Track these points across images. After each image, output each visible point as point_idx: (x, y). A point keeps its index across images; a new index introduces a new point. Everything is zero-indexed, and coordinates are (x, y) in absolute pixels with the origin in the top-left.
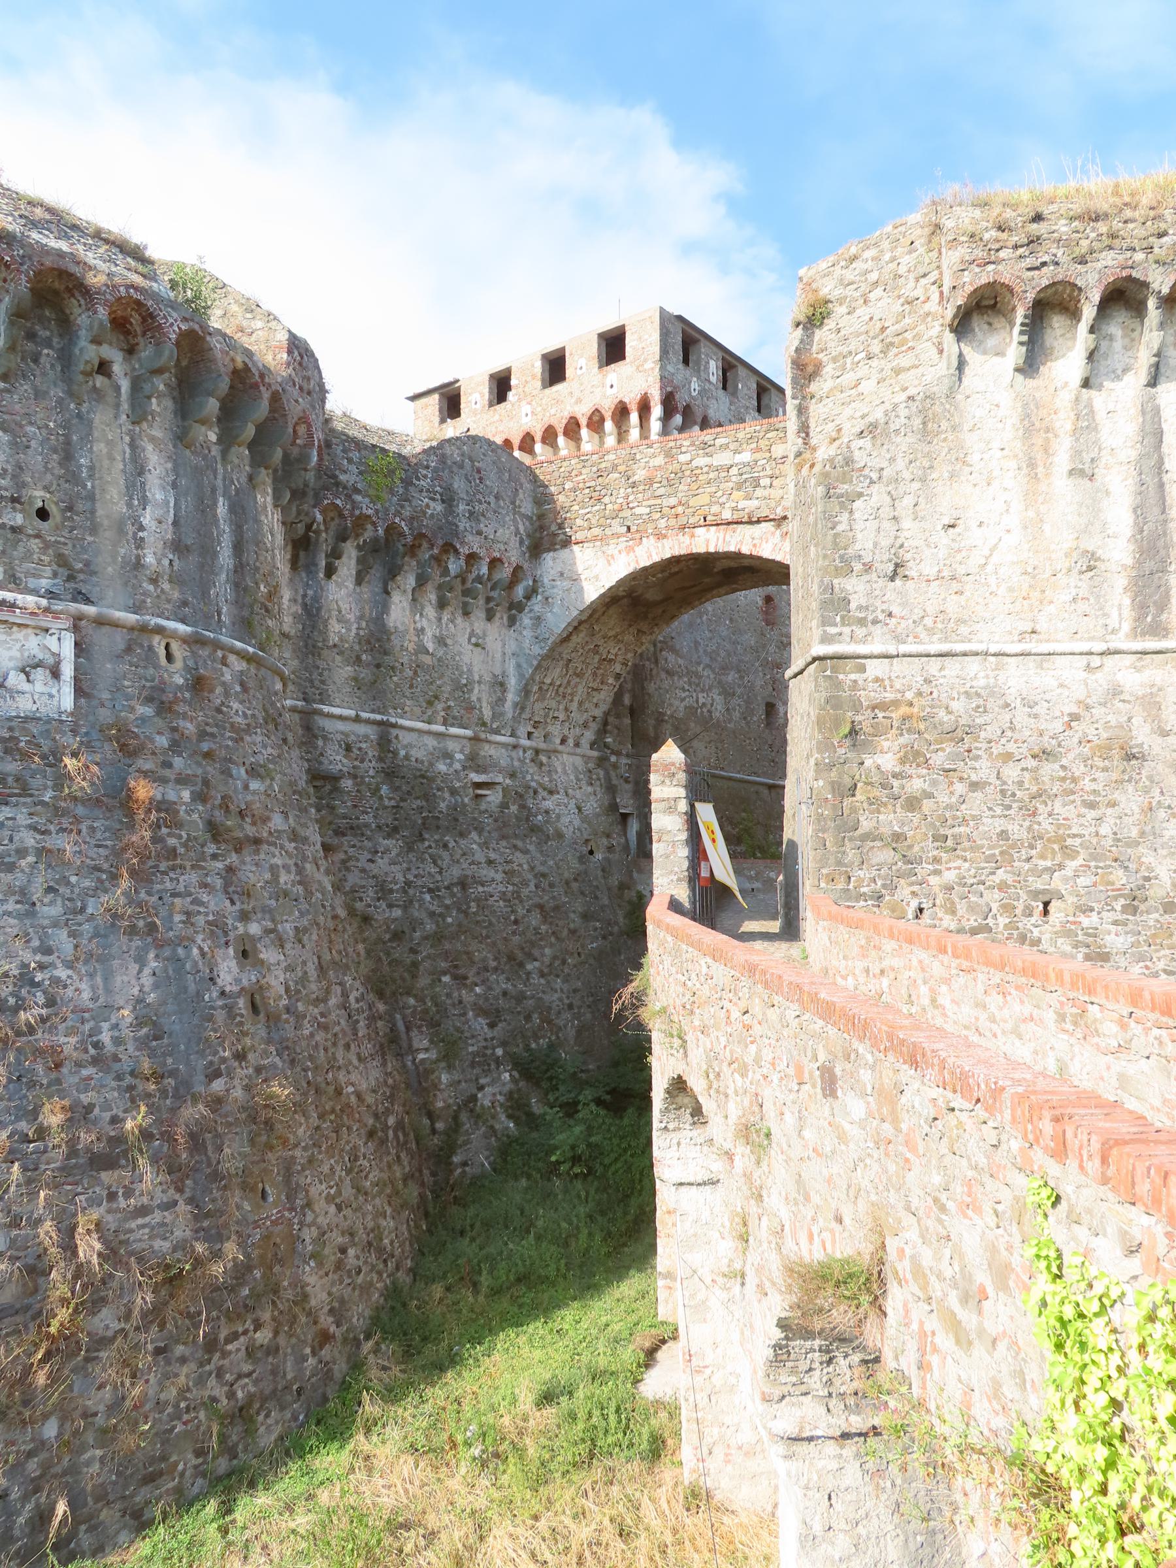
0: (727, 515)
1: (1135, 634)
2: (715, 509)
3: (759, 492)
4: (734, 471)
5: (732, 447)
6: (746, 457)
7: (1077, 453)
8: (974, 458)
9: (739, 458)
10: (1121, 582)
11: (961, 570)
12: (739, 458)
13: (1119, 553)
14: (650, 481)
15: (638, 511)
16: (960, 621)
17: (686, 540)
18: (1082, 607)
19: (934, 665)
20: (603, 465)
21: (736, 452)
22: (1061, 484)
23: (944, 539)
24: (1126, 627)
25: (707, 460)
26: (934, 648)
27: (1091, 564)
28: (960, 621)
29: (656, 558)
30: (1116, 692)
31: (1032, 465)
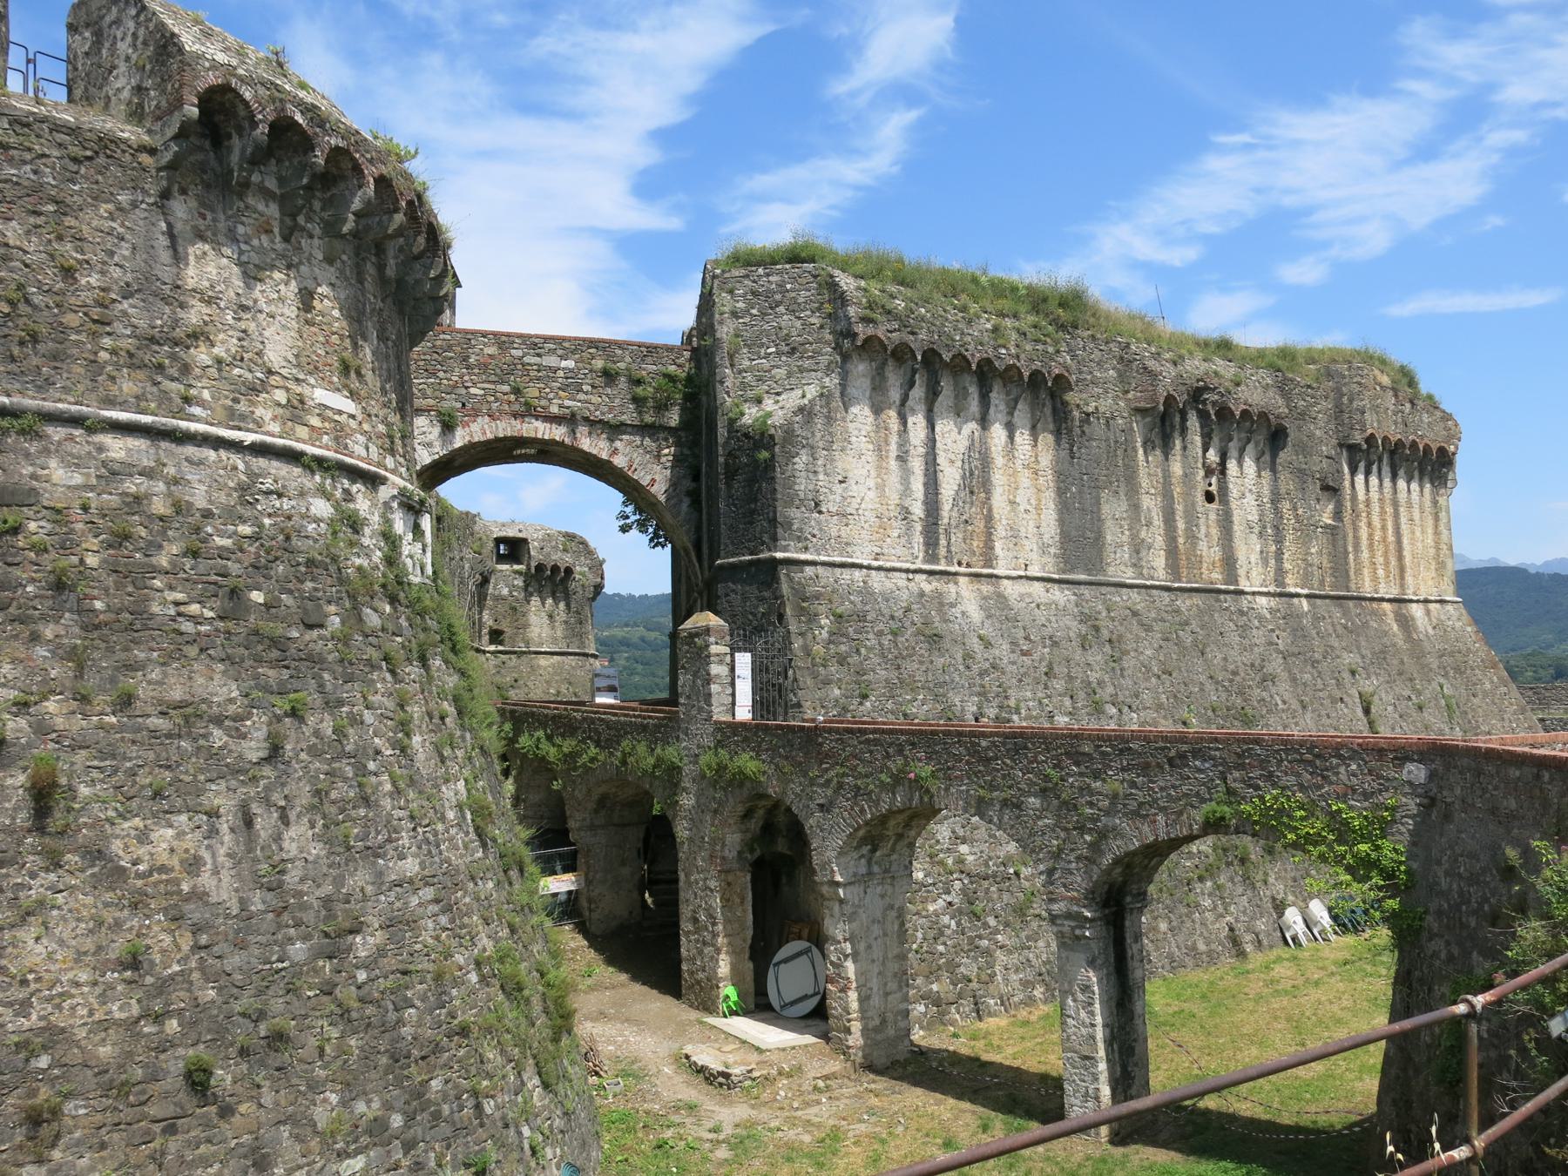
0: (554, 409)
1: (926, 561)
2: (544, 402)
3: (581, 396)
4: (561, 373)
5: (560, 352)
6: (570, 364)
7: (900, 446)
8: (853, 439)
9: (564, 364)
10: (918, 527)
11: (849, 510)
12: (564, 364)
13: (918, 510)
14: (484, 367)
15: (473, 391)
16: (847, 544)
17: (517, 424)
18: (903, 540)
19: (838, 571)
20: (439, 343)
21: (562, 357)
22: (893, 464)
23: (838, 489)
24: (921, 555)
25: (537, 360)
26: (838, 559)
27: (906, 513)
28: (847, 544)
29: (490, 436)
30: (922, 594)
31: (880, 450)
